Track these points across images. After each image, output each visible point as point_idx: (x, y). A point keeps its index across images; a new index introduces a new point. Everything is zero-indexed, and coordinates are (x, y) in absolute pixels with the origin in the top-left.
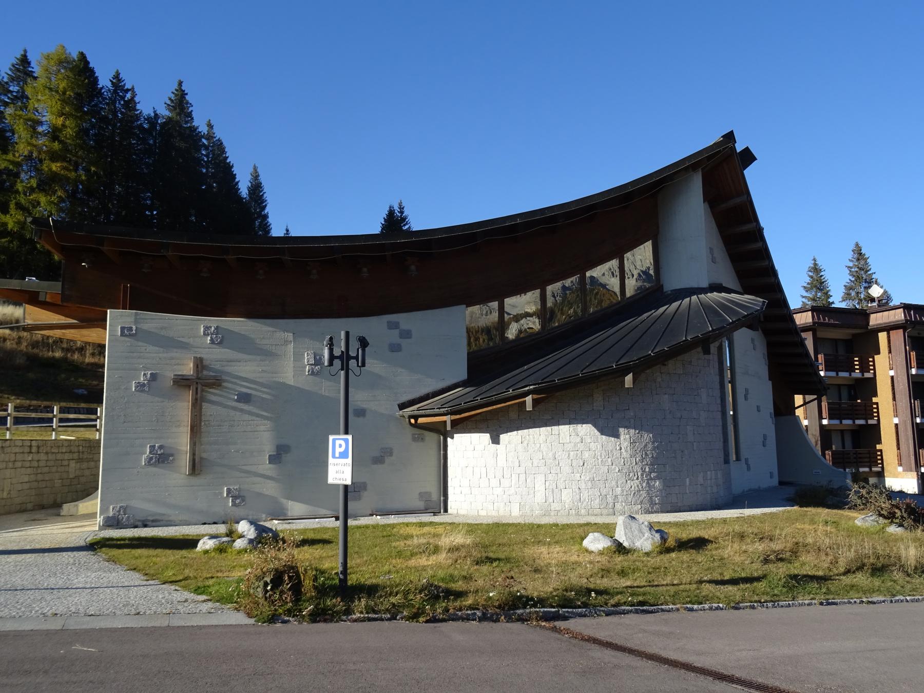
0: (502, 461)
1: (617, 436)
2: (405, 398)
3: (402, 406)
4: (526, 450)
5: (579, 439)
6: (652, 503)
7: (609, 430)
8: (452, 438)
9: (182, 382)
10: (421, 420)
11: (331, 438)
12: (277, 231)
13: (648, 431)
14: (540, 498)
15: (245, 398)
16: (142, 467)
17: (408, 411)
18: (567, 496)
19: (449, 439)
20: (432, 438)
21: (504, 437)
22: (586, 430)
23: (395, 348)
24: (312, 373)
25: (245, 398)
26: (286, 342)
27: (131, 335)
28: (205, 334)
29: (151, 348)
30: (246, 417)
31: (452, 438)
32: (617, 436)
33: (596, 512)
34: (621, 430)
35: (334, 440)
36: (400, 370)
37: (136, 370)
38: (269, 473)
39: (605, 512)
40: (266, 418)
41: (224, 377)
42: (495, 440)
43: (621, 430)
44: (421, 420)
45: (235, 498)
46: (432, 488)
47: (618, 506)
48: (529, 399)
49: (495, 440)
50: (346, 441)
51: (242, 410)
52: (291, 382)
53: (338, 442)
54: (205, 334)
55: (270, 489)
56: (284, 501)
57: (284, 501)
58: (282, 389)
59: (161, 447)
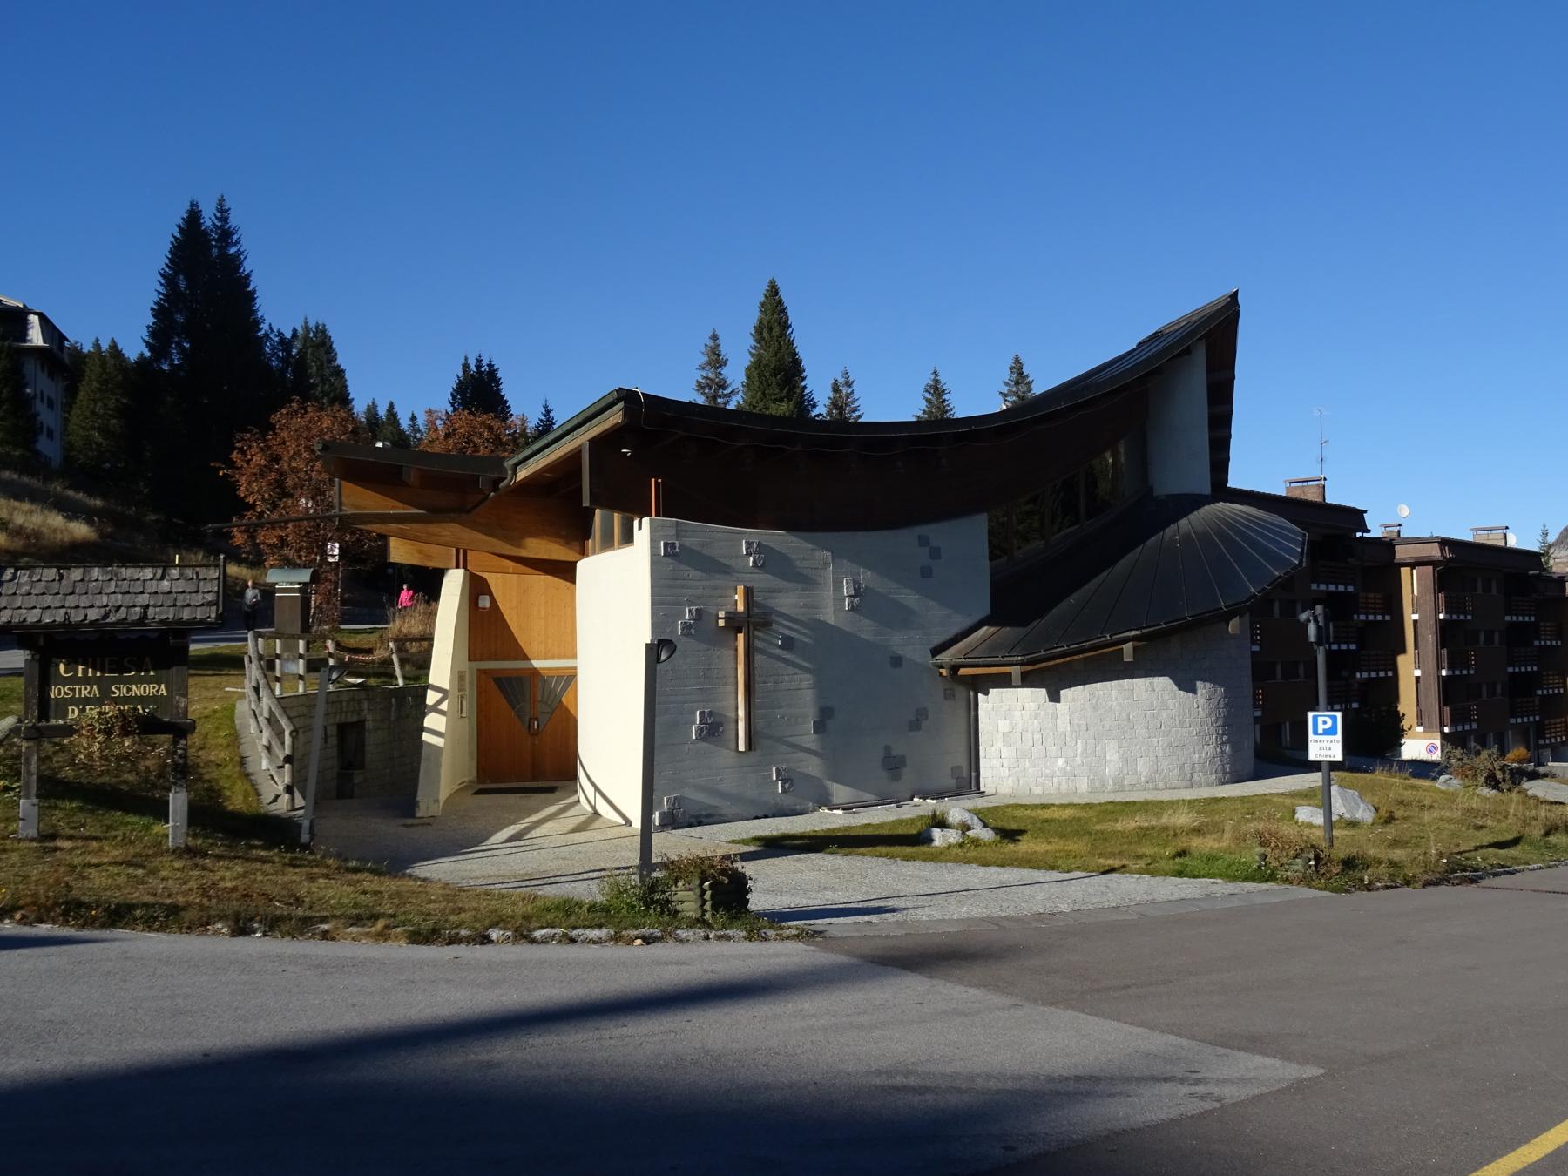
0: (1063, 725)
1: (1194, 691)
2: (937, 640)
3: (936, 651)
4: (1095, 708)
5: (1155, 696)
6: (1225, 773)
7: (1187, 685)
8: (987, 694)
9: (735, 623)
10: (962, 671)
11: (1310, 715)
12: (1230, 485)
13: (1221, 685)
14: (1110, 771)
15: (788, 644)
16: (693, 742)
17: (945, 657)
18: (1143, 767)
19: (980, 696)
20: (961, 692)
21: (1065, 694)
22: (1163, 683)
23: (926, 572)
24: (853, 608)
25: (788, 644)
26: (826, 564)
27: (674, 556)
28: (748, 554)
29: (694, 573)
30: (791, 670)
31: (987, 694)
32: (1194, 691)
33: (1175, 784)
34: (1199, 684)
35: (1315, 718)
36: (931, 603)
37: (679, 604)
38: (813, 746)
39: (1183, 784)
40: (806, 670)
41: (774, 618)
42: (1054, 697)
43: (1199, 684)
44: (962, 671)
45: (784, 781)
46: (962, 761)
47: (1195, 777)
48: (1128, 648)
49: (1054, 697)
50: (1334, 718)
51: (785, 661)
52: (831, 620)
53: (1320, 720)
54: (748, 554)
55: (812, 766)
56: (828, 783)
57: (828, 783)
58: (820, 627)
59: (710, 713)
